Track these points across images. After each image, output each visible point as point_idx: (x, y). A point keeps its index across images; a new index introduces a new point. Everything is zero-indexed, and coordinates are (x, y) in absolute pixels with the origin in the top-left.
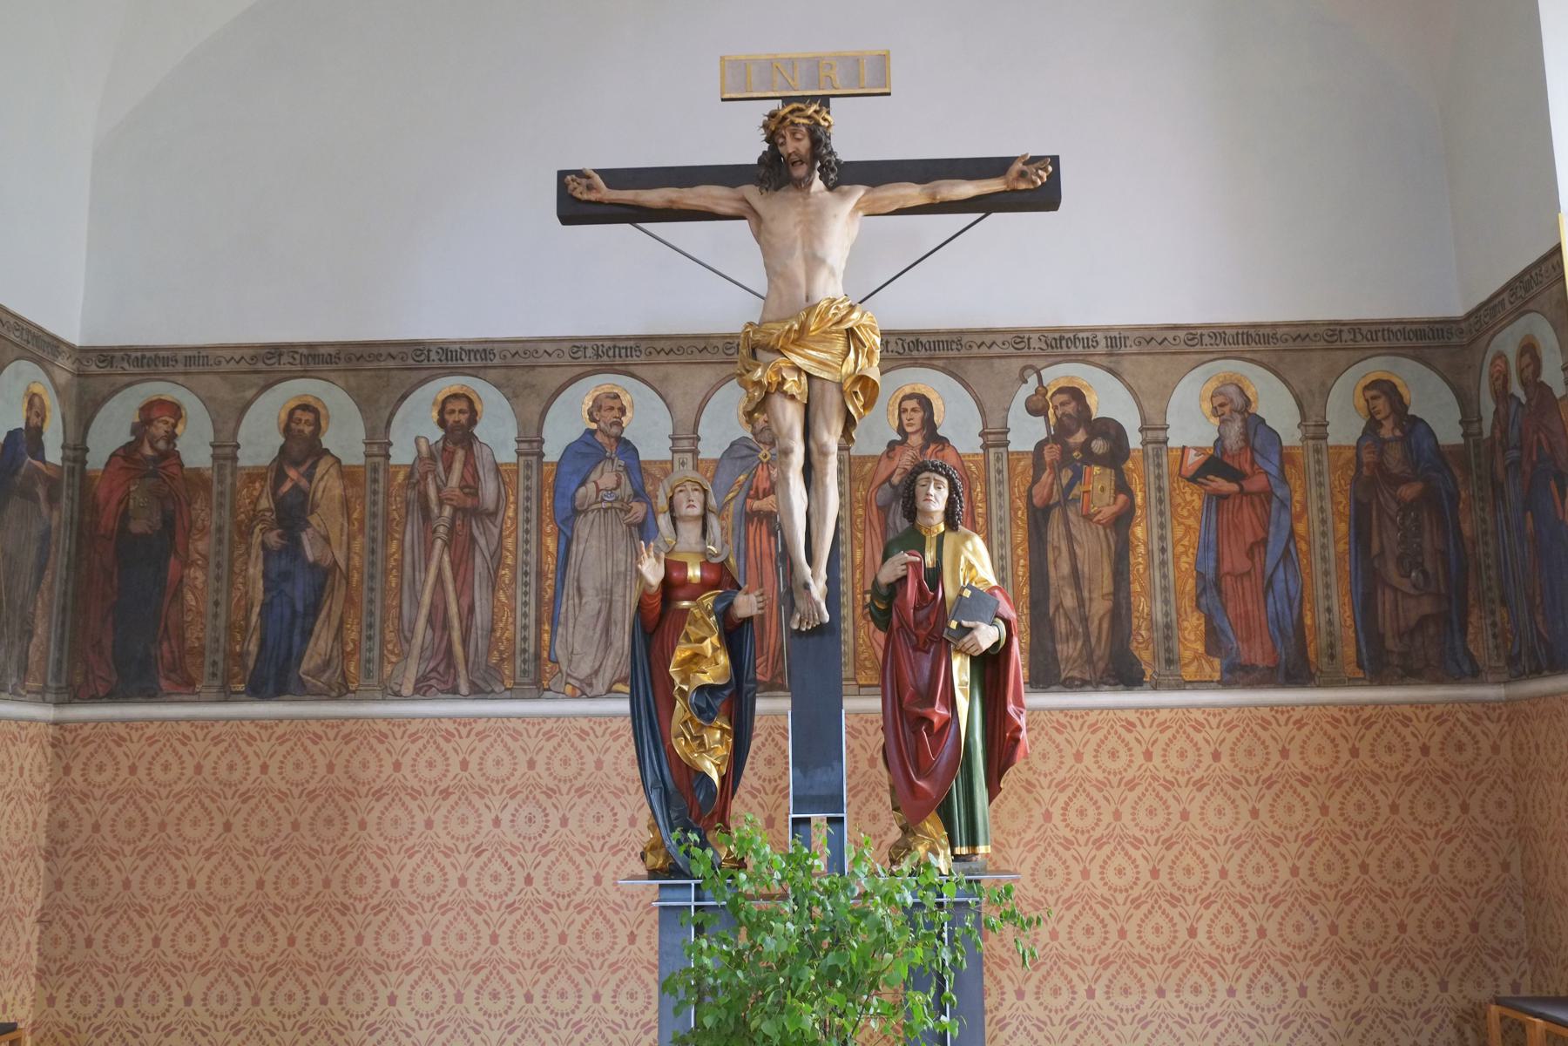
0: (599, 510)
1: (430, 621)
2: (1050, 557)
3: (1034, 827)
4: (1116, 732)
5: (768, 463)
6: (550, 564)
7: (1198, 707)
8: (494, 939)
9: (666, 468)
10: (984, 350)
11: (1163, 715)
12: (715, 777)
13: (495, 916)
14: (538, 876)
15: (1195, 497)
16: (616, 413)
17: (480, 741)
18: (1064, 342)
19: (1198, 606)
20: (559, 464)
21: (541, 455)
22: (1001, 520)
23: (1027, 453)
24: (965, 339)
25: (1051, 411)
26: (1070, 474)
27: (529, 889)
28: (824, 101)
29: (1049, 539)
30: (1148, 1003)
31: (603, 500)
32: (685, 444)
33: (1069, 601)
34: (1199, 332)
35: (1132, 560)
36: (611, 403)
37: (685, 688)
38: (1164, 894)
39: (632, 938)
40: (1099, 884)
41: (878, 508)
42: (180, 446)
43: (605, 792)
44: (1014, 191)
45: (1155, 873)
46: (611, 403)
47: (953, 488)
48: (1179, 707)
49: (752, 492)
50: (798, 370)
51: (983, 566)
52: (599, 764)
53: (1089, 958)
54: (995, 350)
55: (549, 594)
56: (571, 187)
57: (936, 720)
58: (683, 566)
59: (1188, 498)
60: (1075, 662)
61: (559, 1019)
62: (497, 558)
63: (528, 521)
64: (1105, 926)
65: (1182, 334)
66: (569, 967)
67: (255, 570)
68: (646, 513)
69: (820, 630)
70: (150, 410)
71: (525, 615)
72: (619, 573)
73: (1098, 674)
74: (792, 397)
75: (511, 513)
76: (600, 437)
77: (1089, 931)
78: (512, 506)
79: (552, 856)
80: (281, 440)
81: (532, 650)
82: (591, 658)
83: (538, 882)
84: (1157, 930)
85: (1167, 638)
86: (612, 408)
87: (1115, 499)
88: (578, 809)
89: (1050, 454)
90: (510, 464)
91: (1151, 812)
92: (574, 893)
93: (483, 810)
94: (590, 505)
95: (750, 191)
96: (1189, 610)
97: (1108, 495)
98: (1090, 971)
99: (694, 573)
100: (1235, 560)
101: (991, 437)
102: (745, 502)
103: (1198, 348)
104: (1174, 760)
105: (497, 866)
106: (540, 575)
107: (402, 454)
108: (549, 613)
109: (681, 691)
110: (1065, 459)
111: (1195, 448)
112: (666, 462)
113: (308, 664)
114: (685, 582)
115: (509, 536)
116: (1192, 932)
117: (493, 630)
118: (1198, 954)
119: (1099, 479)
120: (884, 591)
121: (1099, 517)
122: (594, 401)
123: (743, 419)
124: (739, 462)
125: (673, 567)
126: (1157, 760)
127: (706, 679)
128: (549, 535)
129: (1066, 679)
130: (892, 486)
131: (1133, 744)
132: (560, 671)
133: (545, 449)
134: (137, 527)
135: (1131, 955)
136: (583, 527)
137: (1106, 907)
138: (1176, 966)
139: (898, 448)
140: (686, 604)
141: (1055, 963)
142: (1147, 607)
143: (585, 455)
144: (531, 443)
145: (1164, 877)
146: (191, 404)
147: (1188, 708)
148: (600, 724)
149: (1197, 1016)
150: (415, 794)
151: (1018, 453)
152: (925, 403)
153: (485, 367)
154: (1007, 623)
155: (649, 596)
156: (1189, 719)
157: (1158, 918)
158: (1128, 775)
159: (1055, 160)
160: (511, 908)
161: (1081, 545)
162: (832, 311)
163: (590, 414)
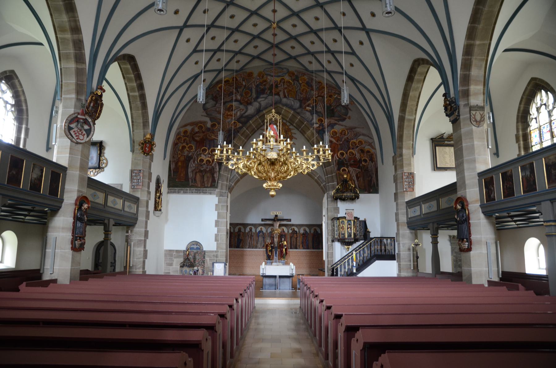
62: (253, 239)
67: (236, 239)
100: (304, 241)
107: (247, 231)
108: (257, 243)
110: (293, 233)
119: (295, 235)
125: (268, 243)
136: (259, 237)
144: (256, 231)
159: (291, 219)
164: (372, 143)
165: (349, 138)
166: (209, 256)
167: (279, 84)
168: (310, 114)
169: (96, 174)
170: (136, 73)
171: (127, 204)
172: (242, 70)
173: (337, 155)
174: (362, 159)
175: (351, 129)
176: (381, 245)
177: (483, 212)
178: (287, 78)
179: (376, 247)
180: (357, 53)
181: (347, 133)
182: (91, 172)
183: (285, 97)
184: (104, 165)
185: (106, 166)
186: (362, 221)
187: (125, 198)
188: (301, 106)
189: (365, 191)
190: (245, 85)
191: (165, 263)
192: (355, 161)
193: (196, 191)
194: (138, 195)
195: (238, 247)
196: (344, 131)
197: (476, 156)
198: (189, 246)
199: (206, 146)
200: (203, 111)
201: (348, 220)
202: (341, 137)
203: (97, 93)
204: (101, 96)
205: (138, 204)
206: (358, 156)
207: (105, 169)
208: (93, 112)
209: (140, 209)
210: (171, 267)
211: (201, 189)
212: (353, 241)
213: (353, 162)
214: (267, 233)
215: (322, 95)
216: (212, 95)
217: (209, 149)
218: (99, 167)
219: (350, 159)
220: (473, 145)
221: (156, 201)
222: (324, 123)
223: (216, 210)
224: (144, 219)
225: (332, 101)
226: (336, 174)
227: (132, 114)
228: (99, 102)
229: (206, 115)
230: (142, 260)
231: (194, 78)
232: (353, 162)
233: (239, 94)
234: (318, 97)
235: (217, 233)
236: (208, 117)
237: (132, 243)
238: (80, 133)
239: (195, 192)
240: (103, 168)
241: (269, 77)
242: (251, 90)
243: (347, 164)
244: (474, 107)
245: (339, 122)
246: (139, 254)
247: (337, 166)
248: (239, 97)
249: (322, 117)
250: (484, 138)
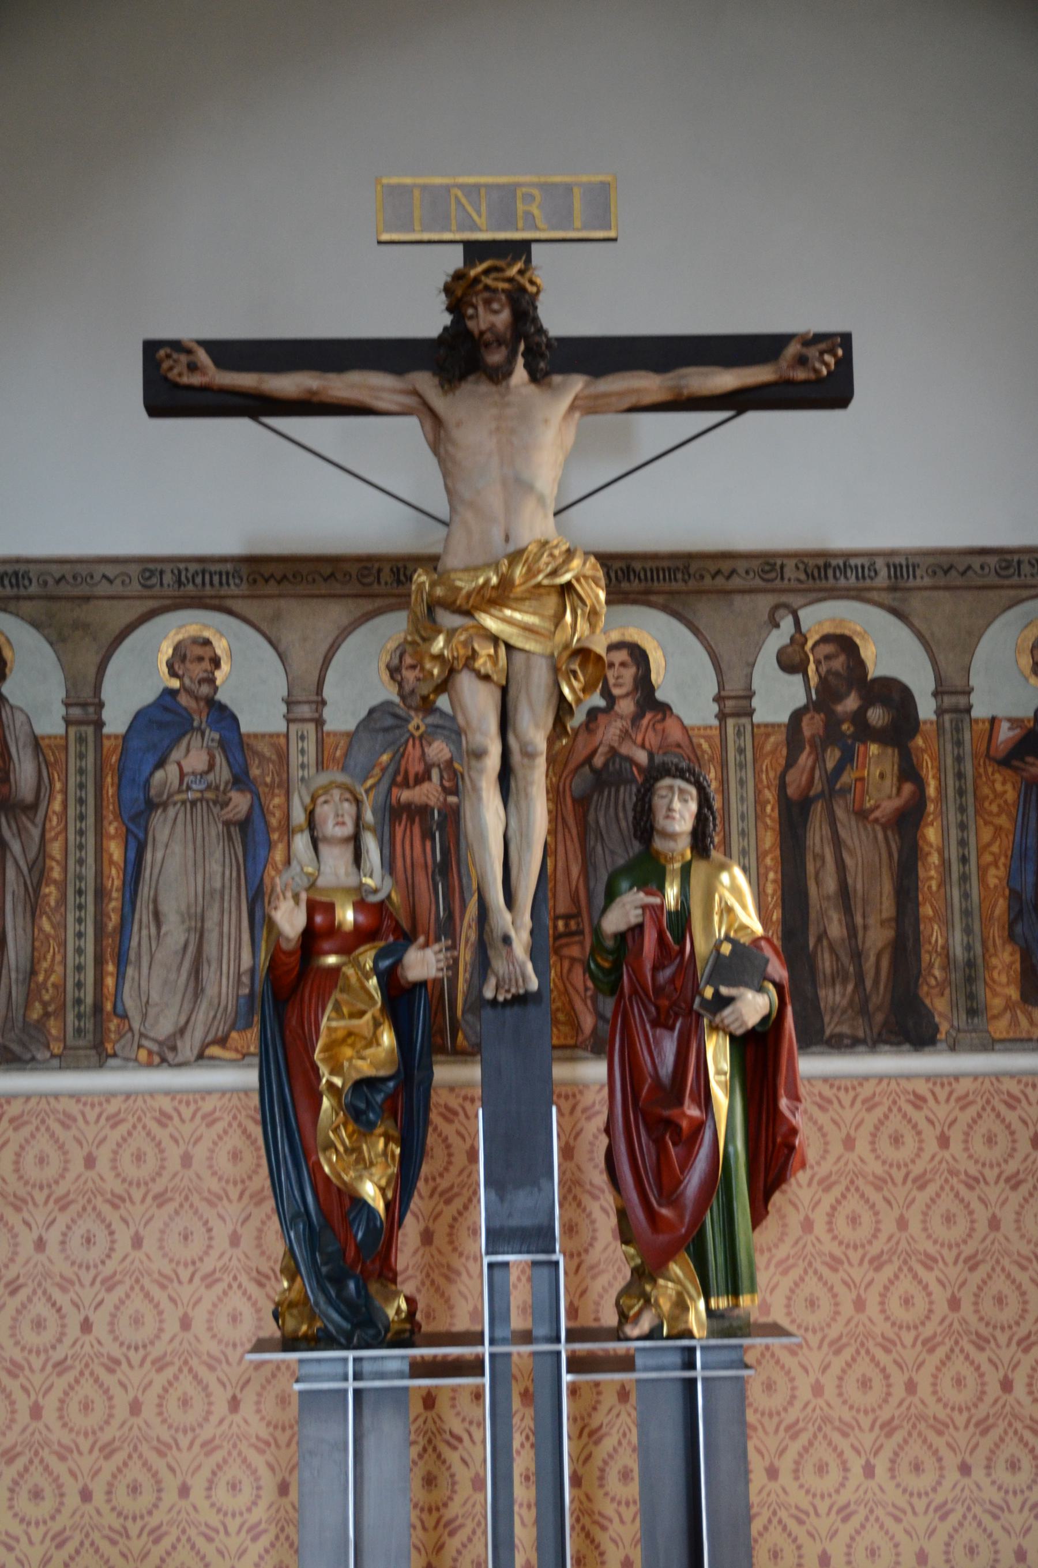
0: (184, 802)
2: (810, 868)
3: (789, 1240)
4: (900, 1109)
5: (421, 737)
6: (114, 878)
7: (1012, 1075)
8: (36, 1412)
10: (720, 581)
11: (963, 1087)
12: (380, 1206)
13: (37, 1379)
14: (100, 1320)
15: (1009, 787)
16: (206, 665)
17: (16, 1129)
18: (830, 573)
19: (1012, 937)
20: (125, 737)
21: (99, 724)
22: (743, 817)
23: (779, 725)
24: (694, 567)
25: (812, 668)
26: (837, 754)
27: (87, 1339)
28: (521, 249)
29: (809, 842)
30: (947, 1484)
31: (189, 788)
32: (305, 711)
33: (836, 930)
34: (1016, 558)
35: (922, 873)
36: (199, 651)
37: (338, 1081)
38: (968, 1332)
39: (234, 1404)
40: (878, 1318)
41: (575, 801)
43: (195, 1199)
44: (789, 382)
45: (954, 1304)
46: (199, 651)
47: (704, 801)
48: (985, 1075)
49: (399, 779)
50: (495, 640)
51: (744, 907)
52: (187, 1160)
53: (866, 1422)
54: (736, 582)
55: (114, 920)
56: (165, 365)
57: (684, 1124)
58: (330, 908)
59: (999, 787)
60: (844, 1012)
61: (129, 1524)
63: (82, 817)
64: (887, 1377)
65: (992, 561)
66: (144, 1448)
68: (251, 807)
69: (522, 1000)
71: (79, 951)
72: (212, 892)
73: (876, 1030)
74: (486, 678)
75: (57, 806)
76: (184, 700)
77: (865, 1384)
78: (59, 798)
79: (120, 1291)
81: (89, 1000)
82: (175, 1009)
83: (100, 1329)
84: (959, 1382)
85: (970, 980)
86: (200, 659)
87: (899, 790)
88: (157, 1224)
90: (55, 737)
91: (949, 1219)
92: (152, 1343)
93: (20, 1228)
94: (170, 796)
95: (425, 381)
96: (998, 942)
97: (889, 784)
98: (868, 1440)
99: (347, 916)
101: (729, 703)
102: (389, 791)
103: (1015, 580)
104: (978, 1147)
105: (40, 1308)
106: (101, 894)
109: (331, 1085)
110: (831, 735)
111: (1010, 720)
112: (278, 735)
114: (332, 930)
115: (56, 838)
116: (1007, 1386)
117: (33, 972)
118: (1016, 1417)
120: (610, 944)
121: (877, 814)
122: (176, 649)
123: (385, 676)
124: (380, 737)
126: (956, 1146)
127: (365, 1068)
128: (113, 838)
129: (832, 1036)
130: (593, 770)
131: (923, 1125)
132: (131, 1029)
133: (106, 715)
135: (921, 1417)
136: (161, 826)
137: (888, 1351)
138: (985, 1432)
139: (602, 719)
140: (332, 960)
141: (820, 1429)
143: (162, 725)
145: (967, 1308)
147: (997, 1076)
148: (188, 1104)
149: (1015, 1503)
151: (766, 725)
152: (639, 656)
153: (18, 598)
154: (779, 987)
155: (284, 953)
156: (999, 1092)
157: (959, 1365)
158: (917, 1170)
160: (61, 1368)
161: (852, 853)
162: (545, 558)
163: (170, 665)
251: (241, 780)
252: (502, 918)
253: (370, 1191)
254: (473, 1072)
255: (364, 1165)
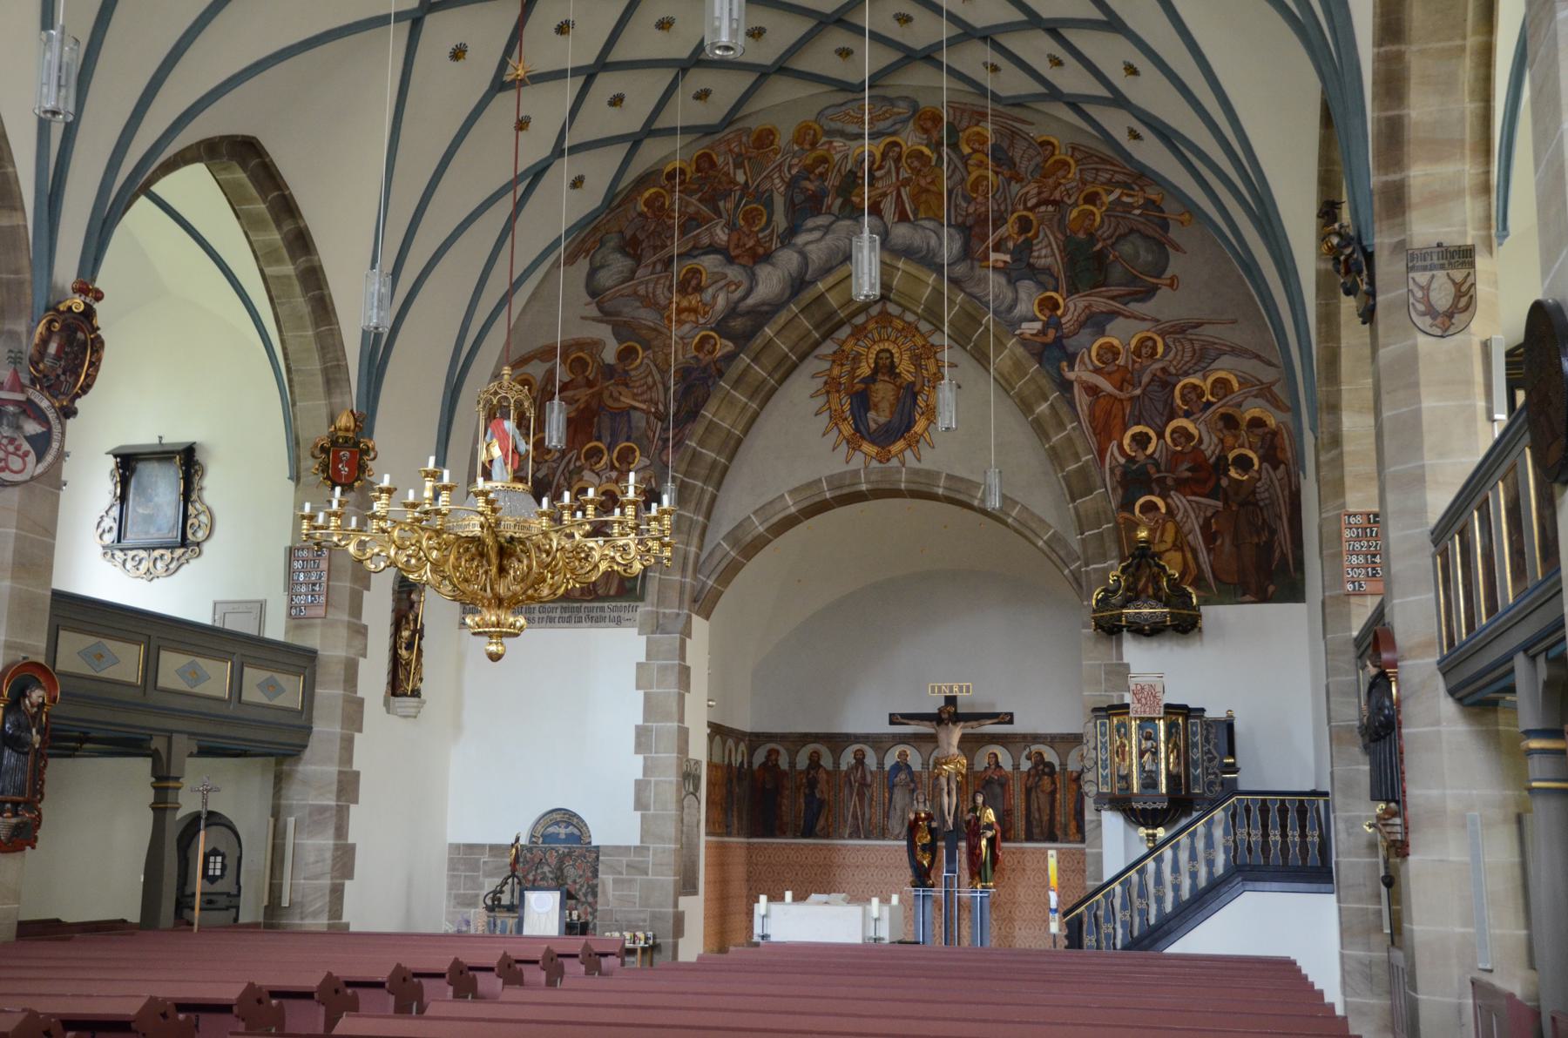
1: (853, 816)
6: (887, 801)
9: (920, 773)
33: (1037, 816)
42: (780, 763)
62: (871, 799)
67: (802, 800)
70: (771, 752)
80: (807, 762)
89: (1033, 772)
104: (1066, 864)
106: (884, 804)
107: (844, 767)
108: (887, 815)
110: (1037, 774)
113: (817, 828)
119: (1046, 780)
134: (767, 787)
136: (896, 790)
142: (1060, 818)
144: (881, 765)
146: (782, 751)
147: (1070, 849)
150: (849, 867)
152: (996, 756)
164: (1273, 384)
165: (1172, 370)
166: (613, 869)
167: (880, 168)
168: (1003, 281)
169: (172, 566)
170: (276, 194)
171: (252, 676)
172: (731, 123)
173: (1120, 447)
174: (1231, 456)
175: (1179, 330)
176: (1265, 826)
177: (1452, 692)
178: (911, 139)
179: (1242, 833)
180: (1130, 24)
181: (1160, 349)
182: (156, 559)
183: (903, 217)
184: (200, 535)
185: (209, 536)
186: (1216, 722)
187: (242, 655)
188: (967, 253)
189: (1244, 595)
190: (746, 182)
191: (449, 895)
192: (1199, 464)
193: (567, 615)
194: (311, 640)
195: (808, 832)
196: (1150, 343)
197: (1429, 460)
198: (540, 829)
199: (599, 439)
200: (589, 299)
201: (1141, 719)
202: (1137, 366)
203: (70, 308)
204: (89, 313)
205: (314, 674)
206: (1210, 447)
207: (206, 547)
208: (60, 371)
209: (319, 691)
210: (473, 910)
211: (585, 604)
212: (1165, 805)
213: (1189, 470)
214: (925, 776)
215: (1057, 195)
216: (621, 232)
217: (610, 448)
218: (184, 543)
219: (1175, 458)
220: (1417, 415)
221: (395, 660)
222: (1064, 315)
223: (638, 687)
224: (337, 729)
225: (1098, 219)
226: (1117, 524)
227: (283, 342)
228: (80, 335)
229: (596, 313)
230: (326, 882)
231: (528, 181)
232: (1187, 470)
233: (723, 221)
234: (1038, 205)
235: (644, 775)
236: (607, 322)
237: (291, 821)
238: (11, 448)
239: (562, 620)
240: (198, 544)
241: (838, 143)
242: (769, 204)
243: (1161, 481)
244: (1424, 254)
245: (1125, 304)
246: (317, 862)
247: (1120, 491)
248: (722, 236)
249: (1056, 290)
250: (1469, 382)
251: (912, 781)
252: (947, 817)
253: (925, 863)
254: (943, 844)
255: (924, 858)
